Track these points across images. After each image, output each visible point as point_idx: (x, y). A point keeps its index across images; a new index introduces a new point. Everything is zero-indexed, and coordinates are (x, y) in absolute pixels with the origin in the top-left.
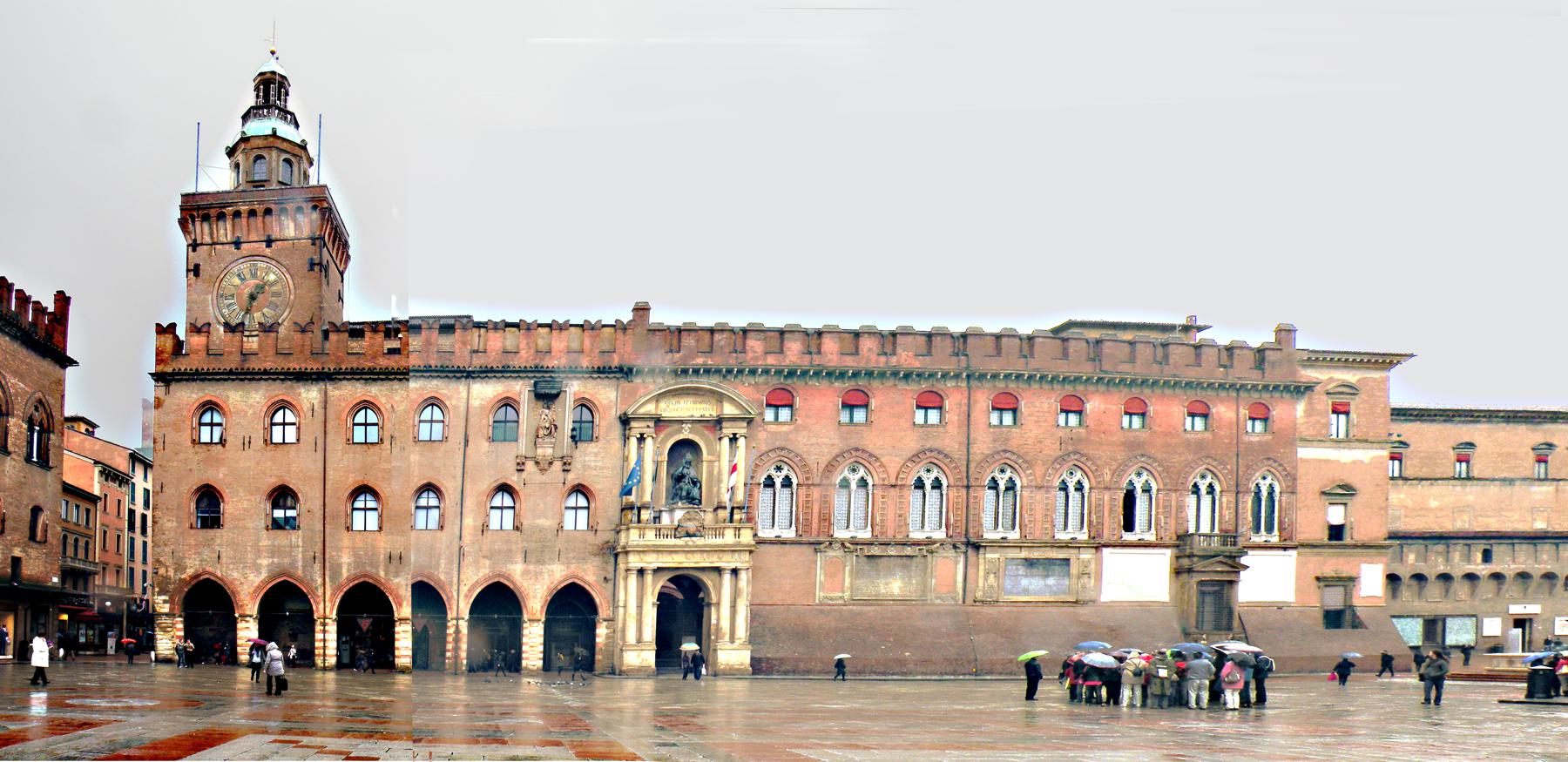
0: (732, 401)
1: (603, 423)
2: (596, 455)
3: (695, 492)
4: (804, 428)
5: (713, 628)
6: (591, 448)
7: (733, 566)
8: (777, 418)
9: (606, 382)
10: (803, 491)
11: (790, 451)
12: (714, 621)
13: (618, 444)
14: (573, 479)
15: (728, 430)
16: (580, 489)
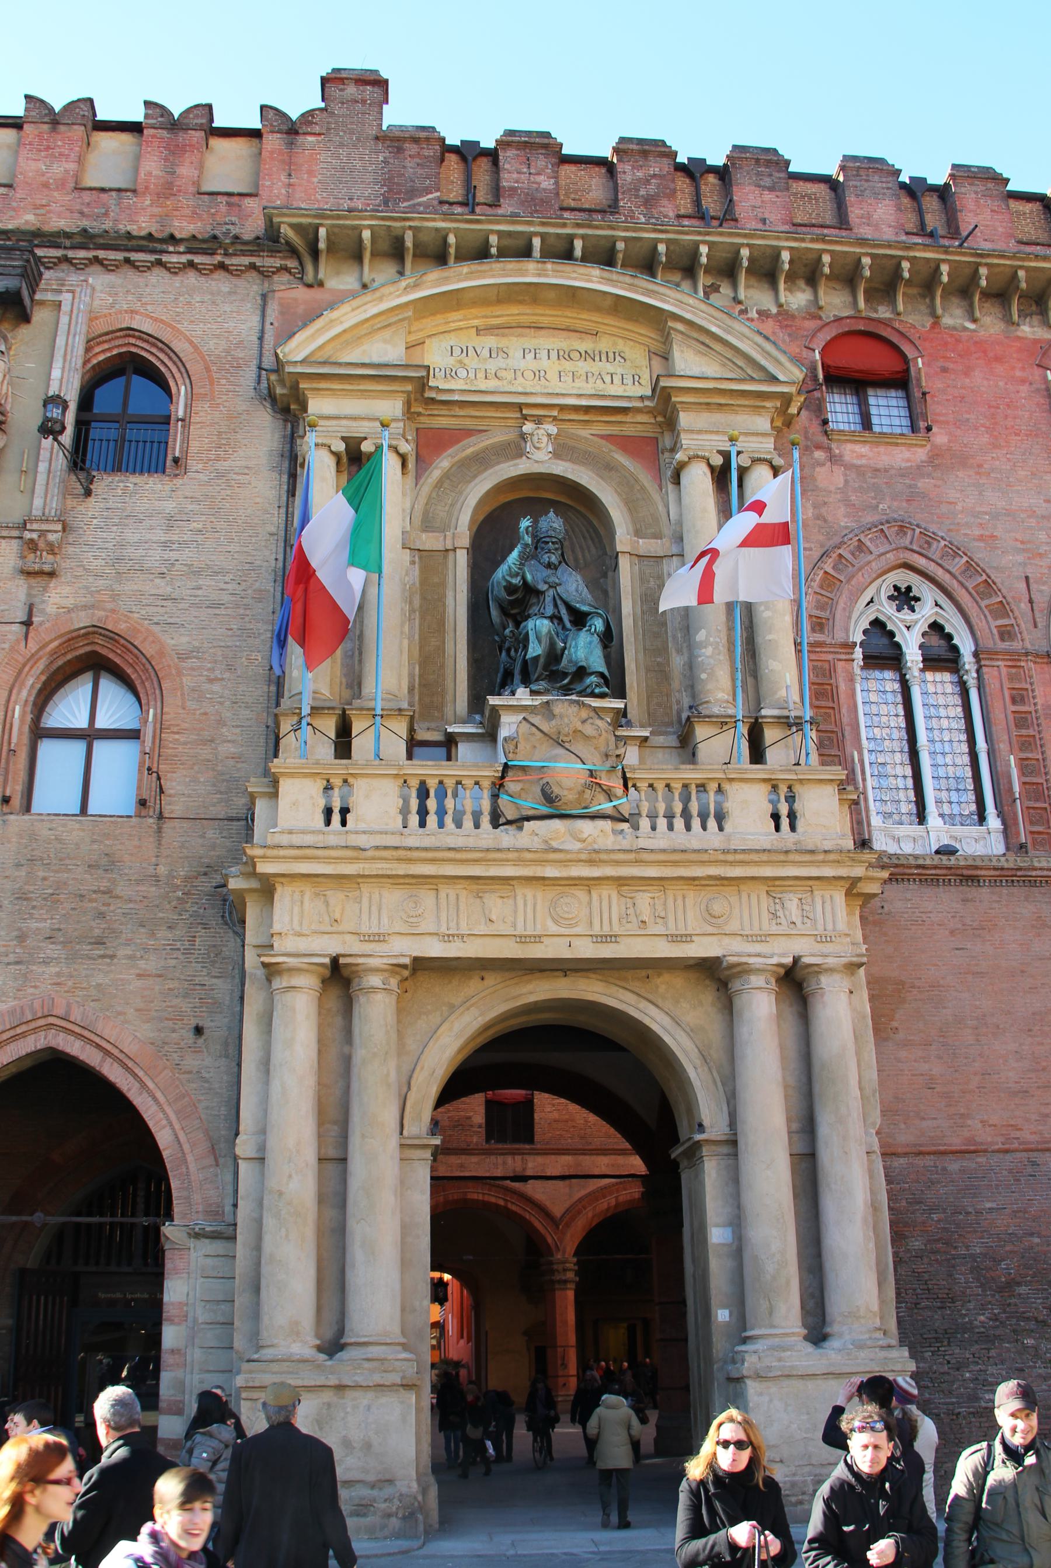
0: (704, 338)
1: (203, 413)
2: (171, 522)
3: (584, 649)
4: (963, 461)
5: (718, 1270)
6: (147, 492)
7: (781, 952)
8: (866, 423)
9: (221, 283)
10: (997, 674)
11: (928, 538)
12: (717, 1235)
13: (264, 488)
14: (63, 604)
15: (700, 434)
16: (95, 658)
